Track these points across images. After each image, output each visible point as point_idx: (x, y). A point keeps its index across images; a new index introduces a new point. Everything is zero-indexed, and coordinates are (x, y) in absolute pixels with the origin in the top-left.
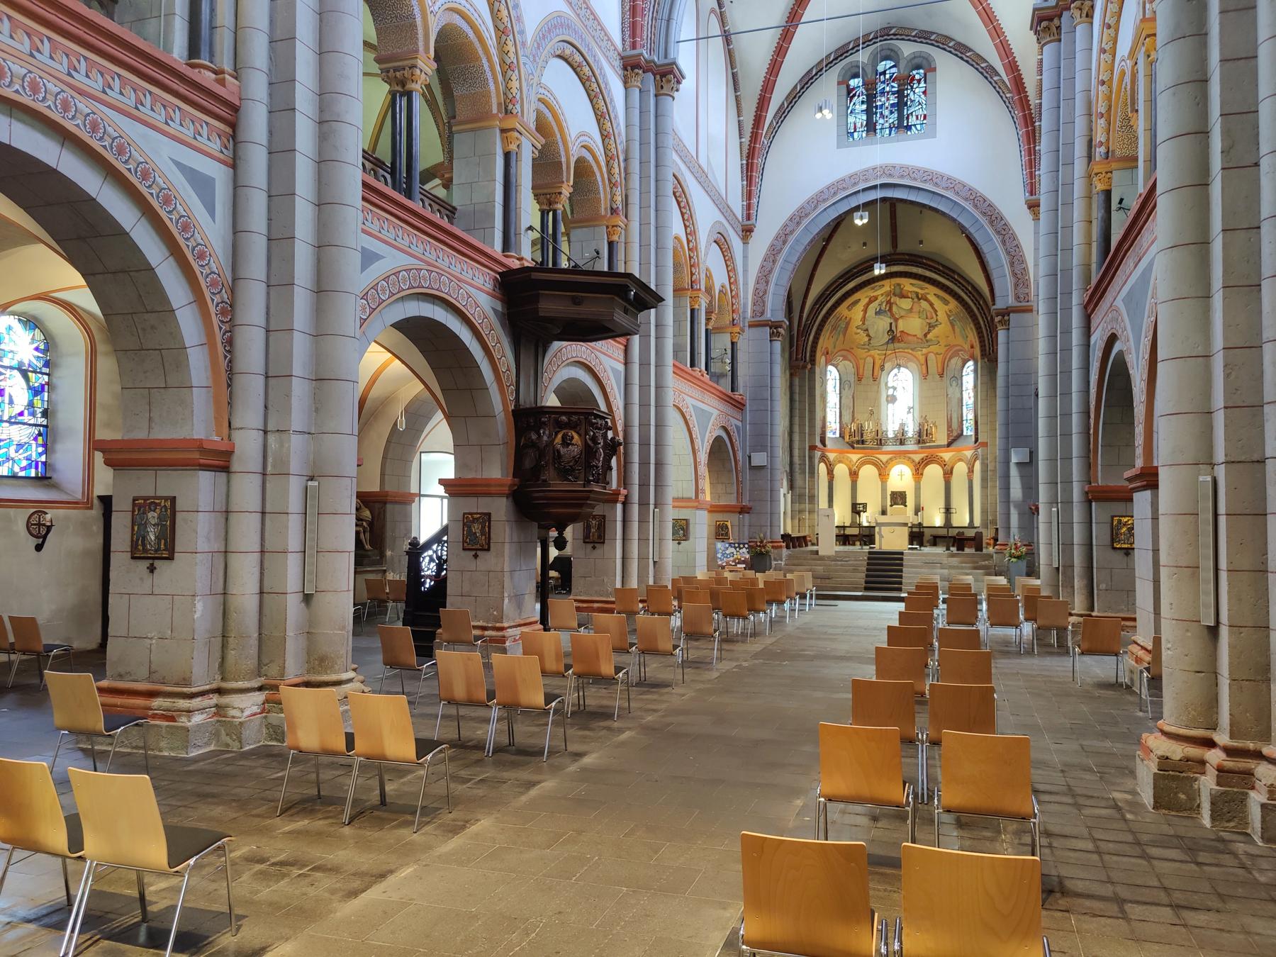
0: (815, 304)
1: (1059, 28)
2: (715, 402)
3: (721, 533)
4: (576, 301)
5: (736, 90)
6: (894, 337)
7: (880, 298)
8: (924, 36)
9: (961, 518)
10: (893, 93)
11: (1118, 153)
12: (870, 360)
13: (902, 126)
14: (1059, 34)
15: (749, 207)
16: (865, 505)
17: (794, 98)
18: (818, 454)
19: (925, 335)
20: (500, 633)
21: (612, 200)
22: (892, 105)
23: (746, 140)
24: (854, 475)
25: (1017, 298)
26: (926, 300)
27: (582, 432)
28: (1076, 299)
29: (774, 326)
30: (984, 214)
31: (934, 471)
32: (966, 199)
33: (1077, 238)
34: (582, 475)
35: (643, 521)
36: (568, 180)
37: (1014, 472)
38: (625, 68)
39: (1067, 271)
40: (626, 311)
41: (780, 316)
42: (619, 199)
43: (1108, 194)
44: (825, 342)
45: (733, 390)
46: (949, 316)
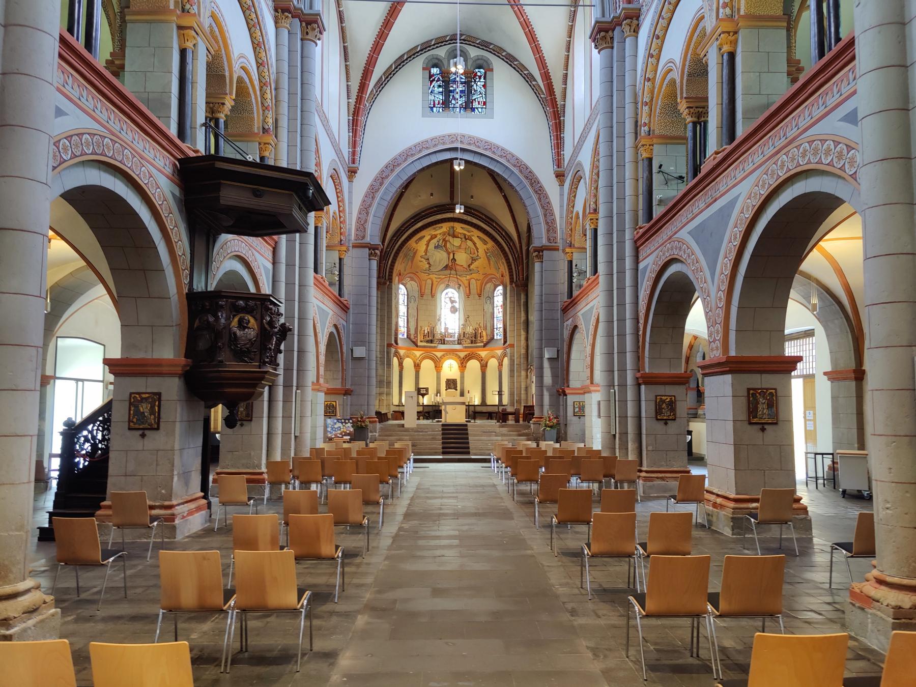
0: (393, 236)
1: (612, 38)
2: (330, 304)
3: (330, 411)
4: (257, 194)
5: (346, 60)
6: (450, 267)
7: (439, 236)
8: (484, 45)
9: (493, 400)
10: (462, 83)
11: (657, 132)
12: (429, 282)
13: (468, 106)
14: (612, 43)
15: (354, 153)
16: (427, 389)
17: (390, 74)
18: (393, 350)
19: (469, 266)
20: (169, 512)
21: (264, 121)
22: (461, 91)
23: (353, 101)
24: (417, 367)
25: (549, 240)
26: (471, 240)
27: (258, 316)
28: (628, 235)
29: (372, 248)
30: (527, 178)
31: (474, 364)
32: (515, 166)
33: (629, 191)
34: (258, 357)
35: (287, 400)
36: (231, 94)
37: (546, 364)
38: (276, 10)
39: (621, 215)
40: (300, 209)
41: (377, 241)
42: (270, 121)
43: (650, 160)
44: (399, 266)
45: (340, 295)
46: (486, 253)
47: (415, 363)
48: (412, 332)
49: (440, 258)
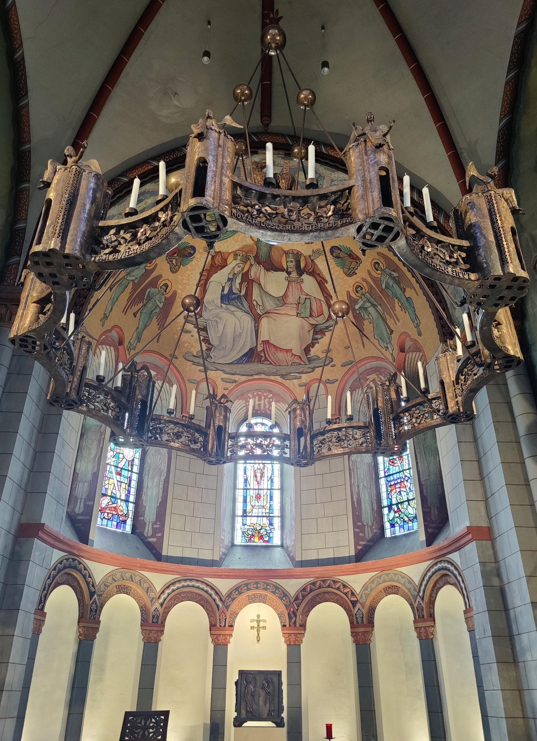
7: (233, 264)
19: (307, 350)
24: (153, 625)
26: (314, 273)
31: (328, 617)
47: (144, 610)
48: (150, 515)
49: (231, 326)
